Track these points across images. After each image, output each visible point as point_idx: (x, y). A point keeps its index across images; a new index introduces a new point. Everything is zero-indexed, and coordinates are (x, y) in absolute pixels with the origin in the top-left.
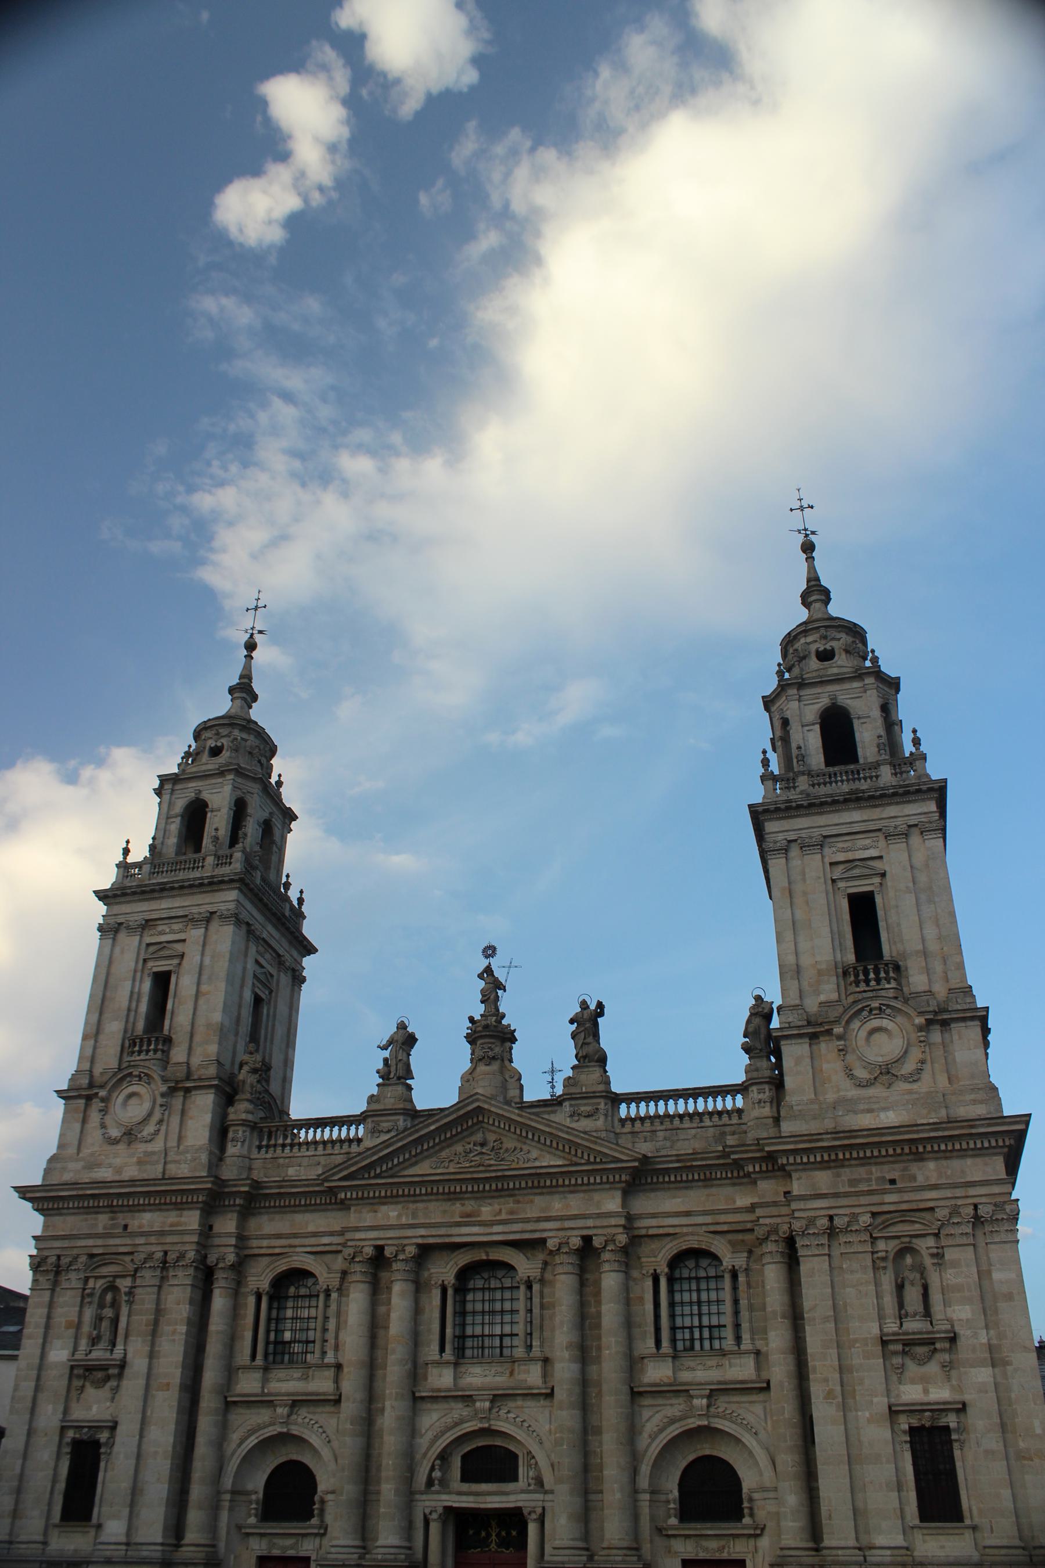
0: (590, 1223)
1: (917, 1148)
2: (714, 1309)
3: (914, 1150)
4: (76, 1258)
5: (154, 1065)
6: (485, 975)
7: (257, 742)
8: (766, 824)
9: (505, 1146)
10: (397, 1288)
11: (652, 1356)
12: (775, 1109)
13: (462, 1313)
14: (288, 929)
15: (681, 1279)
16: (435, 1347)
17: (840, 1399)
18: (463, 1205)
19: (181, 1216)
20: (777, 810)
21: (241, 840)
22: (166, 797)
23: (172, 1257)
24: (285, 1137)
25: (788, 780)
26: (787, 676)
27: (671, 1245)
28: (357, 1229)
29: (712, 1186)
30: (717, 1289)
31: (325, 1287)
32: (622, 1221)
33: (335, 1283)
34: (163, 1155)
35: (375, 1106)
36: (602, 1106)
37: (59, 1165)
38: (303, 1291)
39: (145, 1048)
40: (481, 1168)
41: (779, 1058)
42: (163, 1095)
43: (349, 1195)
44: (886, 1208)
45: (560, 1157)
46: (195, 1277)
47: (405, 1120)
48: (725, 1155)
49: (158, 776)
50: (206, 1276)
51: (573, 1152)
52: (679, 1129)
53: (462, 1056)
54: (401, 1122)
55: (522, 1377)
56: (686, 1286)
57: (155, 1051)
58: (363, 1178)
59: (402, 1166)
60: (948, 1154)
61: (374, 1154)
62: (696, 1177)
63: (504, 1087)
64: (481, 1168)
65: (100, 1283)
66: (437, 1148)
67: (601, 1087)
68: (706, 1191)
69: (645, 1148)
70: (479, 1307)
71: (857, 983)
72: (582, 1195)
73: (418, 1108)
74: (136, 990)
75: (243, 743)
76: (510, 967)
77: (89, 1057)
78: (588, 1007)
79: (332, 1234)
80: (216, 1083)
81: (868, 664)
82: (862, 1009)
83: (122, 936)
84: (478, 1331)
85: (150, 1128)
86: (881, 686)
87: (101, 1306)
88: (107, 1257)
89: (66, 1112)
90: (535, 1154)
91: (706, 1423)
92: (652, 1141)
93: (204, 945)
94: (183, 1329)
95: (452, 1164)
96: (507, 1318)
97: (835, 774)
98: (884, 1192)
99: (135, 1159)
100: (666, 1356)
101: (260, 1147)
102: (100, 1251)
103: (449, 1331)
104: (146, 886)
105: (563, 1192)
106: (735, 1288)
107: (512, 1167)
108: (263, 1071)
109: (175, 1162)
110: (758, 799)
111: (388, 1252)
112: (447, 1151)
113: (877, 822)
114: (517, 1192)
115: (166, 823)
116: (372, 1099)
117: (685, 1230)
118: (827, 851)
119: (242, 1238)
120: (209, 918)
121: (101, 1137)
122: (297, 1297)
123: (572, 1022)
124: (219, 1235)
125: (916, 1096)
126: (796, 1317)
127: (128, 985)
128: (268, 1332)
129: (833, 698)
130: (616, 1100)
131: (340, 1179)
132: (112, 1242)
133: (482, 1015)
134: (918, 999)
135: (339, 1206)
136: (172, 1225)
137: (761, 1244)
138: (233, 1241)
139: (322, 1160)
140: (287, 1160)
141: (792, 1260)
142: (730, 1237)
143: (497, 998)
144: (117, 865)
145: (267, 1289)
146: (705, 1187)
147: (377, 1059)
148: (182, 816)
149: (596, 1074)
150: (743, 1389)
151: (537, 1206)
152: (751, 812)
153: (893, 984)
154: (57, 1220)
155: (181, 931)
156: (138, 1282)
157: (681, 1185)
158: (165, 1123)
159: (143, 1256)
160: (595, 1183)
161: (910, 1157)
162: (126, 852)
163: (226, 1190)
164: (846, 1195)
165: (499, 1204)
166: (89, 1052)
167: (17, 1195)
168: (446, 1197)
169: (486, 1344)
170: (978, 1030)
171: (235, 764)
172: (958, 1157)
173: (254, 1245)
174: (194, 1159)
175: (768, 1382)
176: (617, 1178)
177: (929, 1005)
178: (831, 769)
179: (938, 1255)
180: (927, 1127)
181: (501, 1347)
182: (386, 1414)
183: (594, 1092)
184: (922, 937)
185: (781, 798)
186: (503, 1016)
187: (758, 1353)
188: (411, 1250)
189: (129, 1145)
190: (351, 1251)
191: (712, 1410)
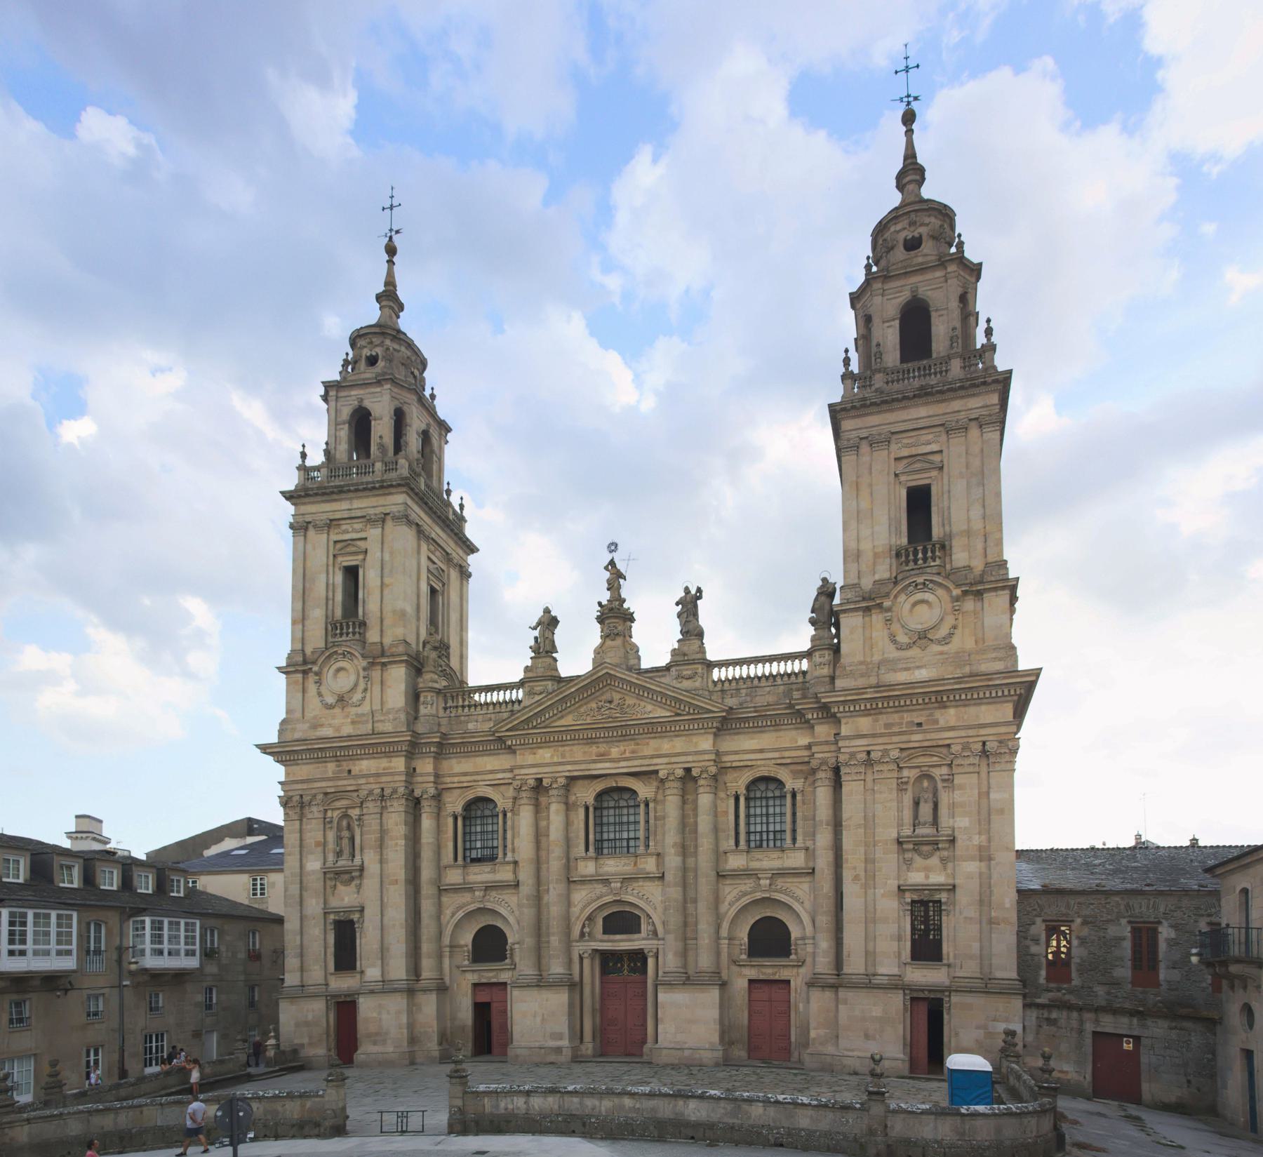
0: (690, 758)
1: (942, 698)
2: (778, 819)
3: (939, 699)
4: (314, 796)
5: (354, 645)
6: (610, 567)
7: (409, 353)
8: (842, 422)
9: (627, 702)
10: (553, 807)
11: (732, 851)
12: (831, 670)
13: (599, 824)
14: (452, 530)
15: (755, 798)
16: (582, 847)
17: (863, 881)
18: (598, 747)
19: (390, 762)
20: (854, 407)
21: (403, 448)
22: (333, 404)
23: (387, 792)
24: (464, 700)
25: (865, 378)
26: (874, 269)
27: (749, 774)
28: (522, 767)
29: (780, 730)
30: (781, 805)
31: (502, 809)
32: (713, 757)
33: (509, 805)
34: (371, 717)
35: (530, 675)
36: (700, 671)
37: (289, 727)
38: (487, 813)
39: (345, 631)
40: (610, 720)
41: (838, 629)
42: (364, 669)
43: (514, 743)
44: (911, 745)
45: (668, 710)
46: (407, 805)
47: (553, 685)
48: (791, 706)
49: (323, 382)
50: (415, 804)
51: (678, 706)
52: (757, 687)
53: (593, 635)
54: (550, 685)
55: (642, 866)
56: (758, 803)
57: (354, 633)
58: (524, 729)
59: (552, 719)
60: (967, 702)
61: (531, 711)
62: (769, 723)
63: (626, 657)
64: (610, 720)
65: (336, 813)
66: (577, 705)
67: (699, 656)
68: (774, 734)
69: (731, 702)
70: (612, 820)
71: (907, 563)
72: (684, 738)
73: (562, 676)
74: (331, 582)
75: (395, 353)
76: (629, 560)
77: (300, 637)
78: (690, 592)
79: (504, 771)
80: (406, 658)
81: (953, 250)
82: (909, 585)
83: (311, 533)
84: (612, 836)
85: (357, 696)
86: (962, 273)
87: (339, 829)
88: (338, 794)
89: (288, 684)
90: (649, 707)
91: (768, 895)
92: (736, 697)
93: (382, 543)
94: (403, 842)
95: (588, 718)
96: (632, 827)
97: (909, 371)
98: (912, 733)
99: (349, 720)
100: (742, 851)
101: (445, 709)
102: (333, 790)
103: (591, 837)
104: (325, 488)
105: (670, 736)
106: (794, 805)
107: (634, 717)
108: (443, 648)
109: (381, 721)
110: (837, 398)
111: (545, 782)
112: (585, 707)
113: (941, 417)
114: (636, 737)
115: (336, 430)
116: (527, 669)
117: (759, 763)
118: (893, 447)
119: (437, 776)
120: (383, 519)
121: (320, 704)
122: (482, 817)
123: (677, 604)
124: (421, 775)
125: (946, 656)
126: (837, 825)
127: (323, 577)
128: (464, 841)
129: (914, 291)
130: (711, 665)
131: (507, 730)
132: (341, 783)
133: (608, 601)
134: (959, 574)
135: (507, 751)
136: (384, 769)
137: (814, 773)
138: (432, 779)
139: (493, 716)
140: (467, 718)
141: (837, 784)
142: (792, 767)
143: (619, 587)
144: (298, 468)
145: (461, 812)
146: (776, 730)
147: (530, 637)
148: (350, 424)
149: (698, 643)
150: (795, 873)
151: (652, 746)
152: (831, 411)
153: (938, 562)
154: (294, 768)
155: (362, 530)
156: (365, 811)
157: (759, 729)
158: (369, 691)
159: (366, 792)
160: (693, 729)
161: (936, 705)
162: (304, 455)
163: (423, 741)
164: (881, 735)
165: (624, 746)
166: (299, 635)
167: (259, 750)
168: (585, 741)
169: (617, 845)
170: (1007, 598)
171: (389, 374)
172: (975, 704)
173: (448, 781)
174: (395, 719)
175: (814, 869)
176: (710, 725)
177: (967, 579)
178: (905, 366)
179: (949, 780)
180: (952, 681)
181: (628, 847)
182: (551, 893)
183: (694, 660)
184: (968, 518)
185: (856, 397)
186: (624, 601)
187: (807, 849)
188: (562, 781)
189: (343, 709)
190: (519, 783)
191: (773, 887)
